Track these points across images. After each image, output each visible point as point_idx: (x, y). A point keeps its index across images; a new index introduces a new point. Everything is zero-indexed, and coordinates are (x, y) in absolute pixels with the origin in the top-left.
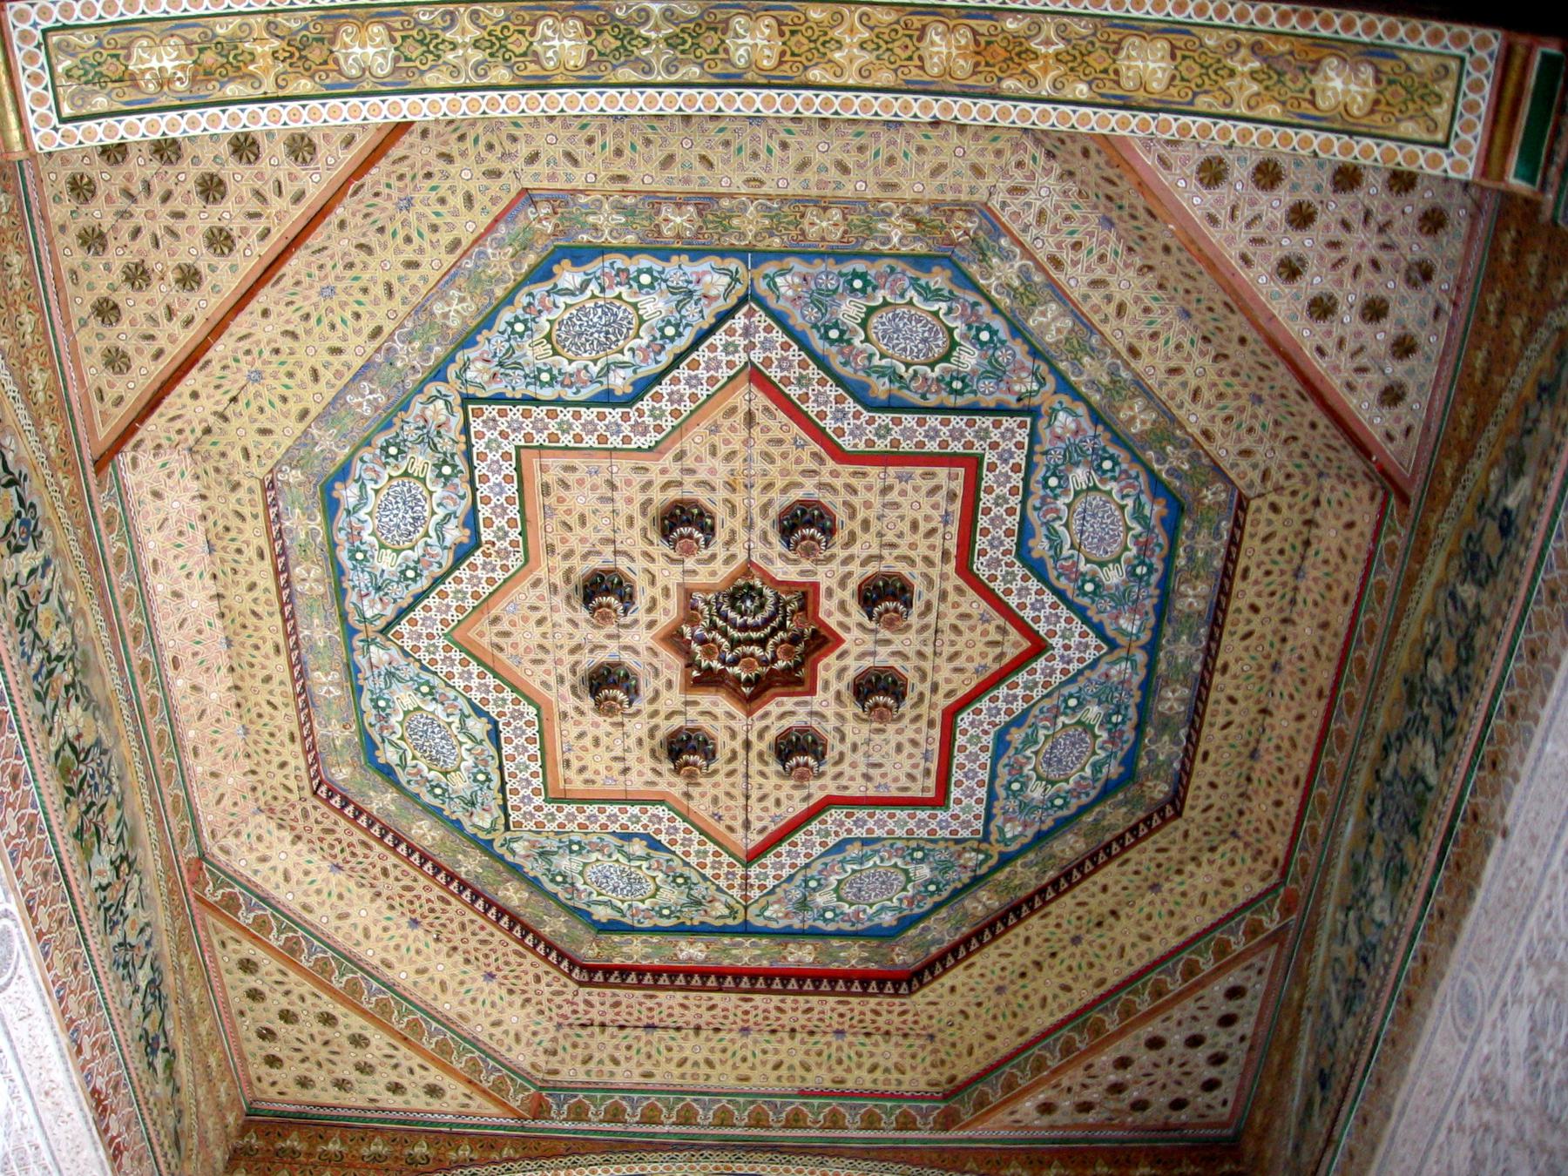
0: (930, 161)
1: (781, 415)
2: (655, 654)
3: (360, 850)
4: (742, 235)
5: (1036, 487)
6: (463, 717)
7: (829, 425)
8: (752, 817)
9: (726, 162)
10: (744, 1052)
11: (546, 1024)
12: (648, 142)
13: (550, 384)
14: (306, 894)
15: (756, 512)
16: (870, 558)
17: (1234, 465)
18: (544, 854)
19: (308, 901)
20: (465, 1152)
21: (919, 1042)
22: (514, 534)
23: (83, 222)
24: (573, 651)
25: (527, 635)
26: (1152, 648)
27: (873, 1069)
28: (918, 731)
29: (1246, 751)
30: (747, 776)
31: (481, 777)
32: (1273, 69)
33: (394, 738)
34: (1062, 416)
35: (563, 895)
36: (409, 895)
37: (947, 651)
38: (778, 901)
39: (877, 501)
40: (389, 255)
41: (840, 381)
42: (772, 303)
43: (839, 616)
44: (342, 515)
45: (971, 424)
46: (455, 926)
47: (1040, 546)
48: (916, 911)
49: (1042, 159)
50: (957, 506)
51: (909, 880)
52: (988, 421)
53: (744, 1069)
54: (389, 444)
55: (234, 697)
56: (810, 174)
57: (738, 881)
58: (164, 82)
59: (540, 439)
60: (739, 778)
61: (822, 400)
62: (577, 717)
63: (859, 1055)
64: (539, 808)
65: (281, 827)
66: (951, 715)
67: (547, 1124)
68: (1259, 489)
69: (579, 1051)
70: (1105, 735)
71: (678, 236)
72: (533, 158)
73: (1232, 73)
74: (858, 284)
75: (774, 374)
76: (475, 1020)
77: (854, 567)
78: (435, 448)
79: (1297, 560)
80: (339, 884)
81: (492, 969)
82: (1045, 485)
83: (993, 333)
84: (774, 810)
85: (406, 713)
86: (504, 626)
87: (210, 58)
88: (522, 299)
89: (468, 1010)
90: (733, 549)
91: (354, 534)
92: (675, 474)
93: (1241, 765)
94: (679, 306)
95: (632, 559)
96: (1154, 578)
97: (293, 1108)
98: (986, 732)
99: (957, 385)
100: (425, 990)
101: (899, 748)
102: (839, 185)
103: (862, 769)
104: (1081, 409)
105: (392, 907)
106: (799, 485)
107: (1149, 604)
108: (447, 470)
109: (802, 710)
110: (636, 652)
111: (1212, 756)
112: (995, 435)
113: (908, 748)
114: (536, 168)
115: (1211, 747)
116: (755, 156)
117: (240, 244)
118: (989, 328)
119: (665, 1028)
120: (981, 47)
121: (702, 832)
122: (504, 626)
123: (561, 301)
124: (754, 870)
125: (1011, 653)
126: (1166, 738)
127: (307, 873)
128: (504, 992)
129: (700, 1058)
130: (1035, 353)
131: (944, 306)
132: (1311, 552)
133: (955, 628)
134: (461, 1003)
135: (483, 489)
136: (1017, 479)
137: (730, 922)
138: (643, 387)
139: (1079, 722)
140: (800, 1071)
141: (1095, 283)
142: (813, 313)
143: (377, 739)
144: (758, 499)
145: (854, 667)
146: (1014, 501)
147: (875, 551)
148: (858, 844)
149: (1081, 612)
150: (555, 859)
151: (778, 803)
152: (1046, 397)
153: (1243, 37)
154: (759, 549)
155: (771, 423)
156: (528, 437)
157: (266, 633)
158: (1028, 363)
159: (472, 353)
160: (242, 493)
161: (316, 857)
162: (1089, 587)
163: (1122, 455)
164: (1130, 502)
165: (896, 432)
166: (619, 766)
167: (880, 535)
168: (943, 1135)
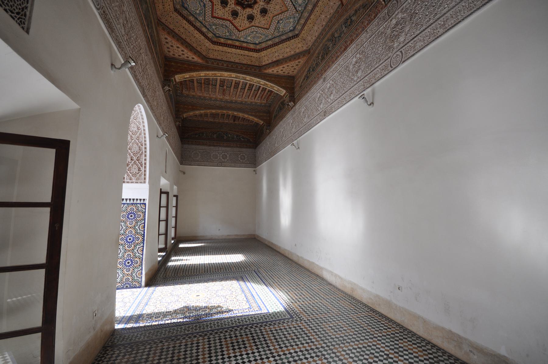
1: (237, 26)
7: (231, 24)
22: (273, 21)
24: (272, 3)
39: (225, 14)
44: (294, 26)
47: (202, 4)
50: (214, 11)
61: (231, 27)
75: (237, 31)
86: (280, 9)
91: (293, 24)
104: (199, 20)
112: (210, 19)
122: (280, 9)
135: (275, 26)
136: (206, 14)
142: (232, 34)
144: (241, 17)
146: (206, 11)
160: (302, 36)
163: (192, 13)
165: (223, 22)
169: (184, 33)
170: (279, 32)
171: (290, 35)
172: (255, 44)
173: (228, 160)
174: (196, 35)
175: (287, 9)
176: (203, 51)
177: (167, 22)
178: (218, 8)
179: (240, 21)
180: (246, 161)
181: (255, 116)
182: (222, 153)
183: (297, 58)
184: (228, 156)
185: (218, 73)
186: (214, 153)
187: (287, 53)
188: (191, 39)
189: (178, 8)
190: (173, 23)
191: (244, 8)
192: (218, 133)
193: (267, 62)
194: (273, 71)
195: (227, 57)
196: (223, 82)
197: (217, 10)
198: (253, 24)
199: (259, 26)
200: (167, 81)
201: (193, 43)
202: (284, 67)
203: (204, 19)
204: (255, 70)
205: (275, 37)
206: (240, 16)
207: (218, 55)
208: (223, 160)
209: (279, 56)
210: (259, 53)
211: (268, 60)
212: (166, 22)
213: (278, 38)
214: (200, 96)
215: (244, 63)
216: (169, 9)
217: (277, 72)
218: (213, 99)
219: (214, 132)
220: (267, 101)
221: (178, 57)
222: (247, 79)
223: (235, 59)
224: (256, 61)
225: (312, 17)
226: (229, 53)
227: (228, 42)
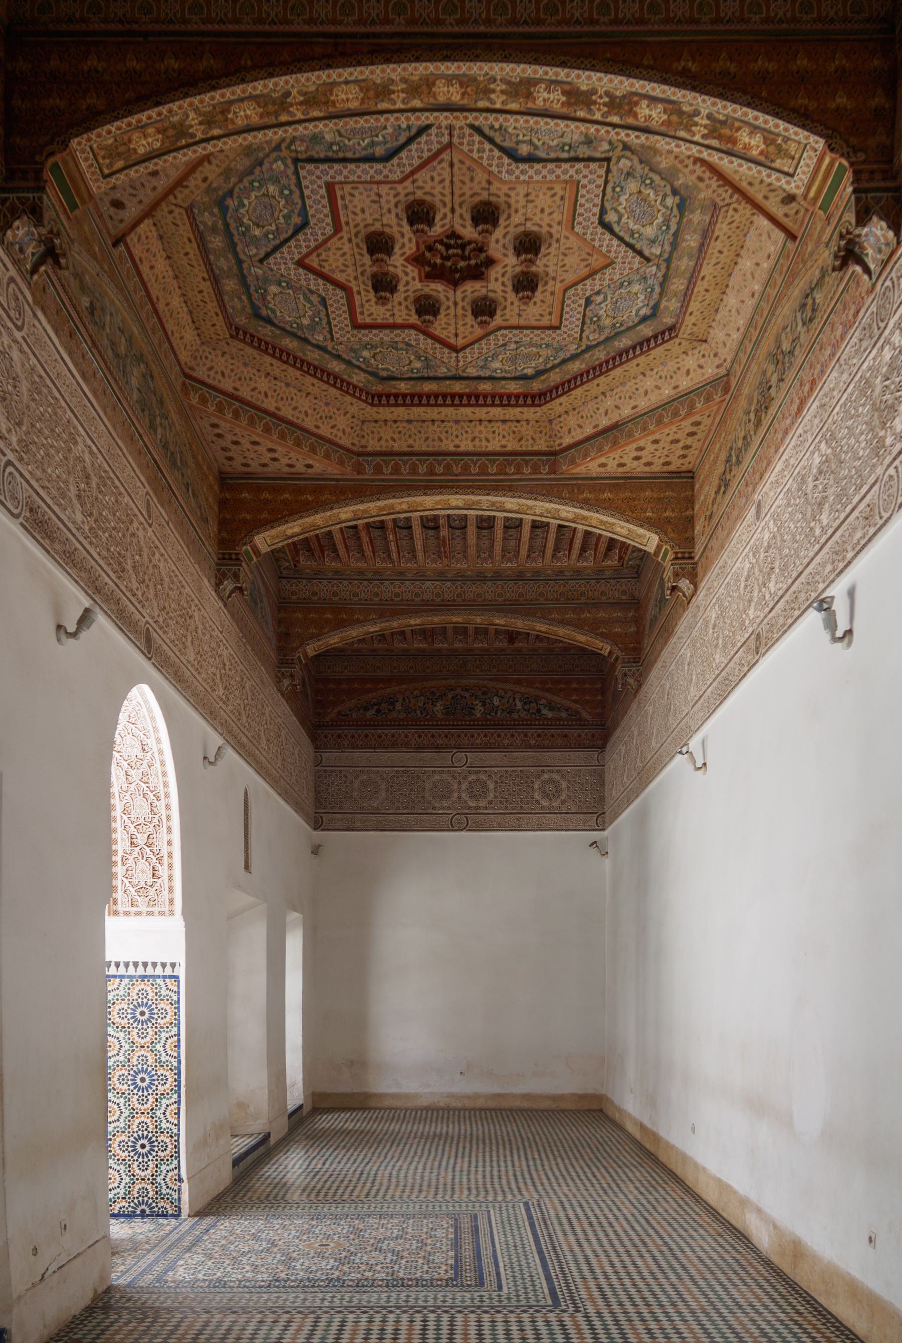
8: (448, 170)
22: (568, 302)
28: (354, 220)
62: (552, 223)
64: (585, 177)
70: (245, 220)
86: (583, 264)
88: (549, 366)
101: (363, 211)
104: (314, 341)
113: (358, 210)
122: (583, 264)
136: (334, 323)
139: (263, 227)
151: (432, 179)
152: (329, 345)
163: (289, 329)
170: (601, 329)
172: (524, 377)
173: (491, 802)
174: (310, 389)
176: (340, 434)
179: (452, 322)
180: (563, 802)
181: (578, 625)
182: (465, 778)
183: (683, 413)
184: (491, 786)
185: (401, 504)
186: (437, 777)
188: (294, 404)
190: (232, 370)
191: (455, 284)
192: (450, 696)
193: (578, 435)
194: (603, 465)
195: (427, 439)
196: (431, 524)
198: (498, 320)
199: (522, 322)
200: (230, 559)
202: (641, 449)
203: (329, 336)
204: (536, 470)
205: (589, 348)
207: (396, 436)
208: (472, 804)
210: (545, 408)
211: (580, 426)
213: (602, 347)
214: (361, 572)
215: (490, 448)
217: (621, 465)
218: (410, 576)
219: (433, 693)
220: (621, 558)
221: (260, 469)
224: (538, 436)
225: (706, 270)
226: (433, 421)
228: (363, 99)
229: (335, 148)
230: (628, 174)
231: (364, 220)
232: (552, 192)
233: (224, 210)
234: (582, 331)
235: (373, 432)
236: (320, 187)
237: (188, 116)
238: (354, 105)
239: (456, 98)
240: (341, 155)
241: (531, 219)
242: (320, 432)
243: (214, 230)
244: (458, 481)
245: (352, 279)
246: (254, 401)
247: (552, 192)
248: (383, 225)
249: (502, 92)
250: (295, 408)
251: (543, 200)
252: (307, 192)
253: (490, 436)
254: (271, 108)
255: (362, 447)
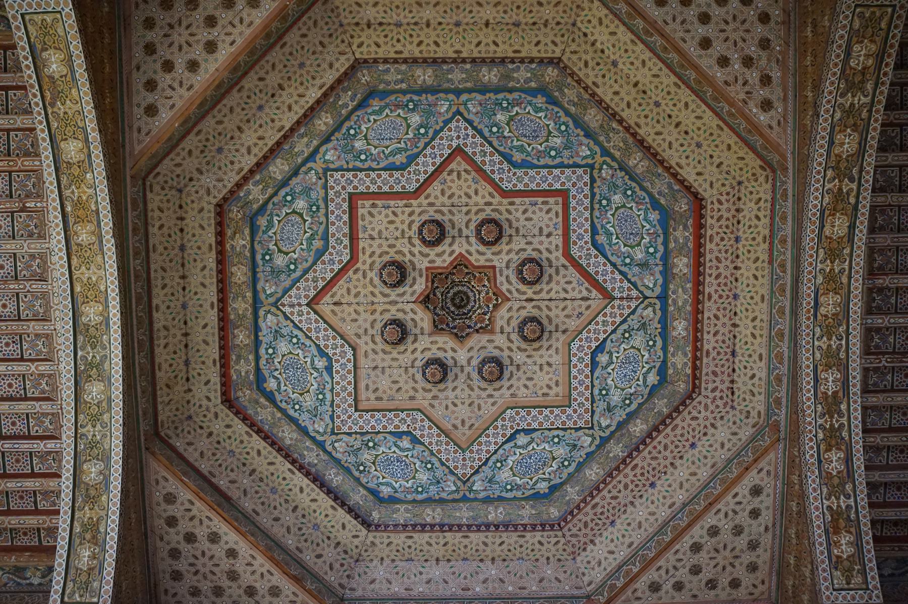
0: (198, 231)
1: (334, 290)
2: (472, 348)
3: (599, 510)
4: (246, 309)
5: (366, 165)
6: (516, 446)
7: (337, 267)
8: (580, 296)
9: (204, 318)
10: (748, 298)
11: (730, 415)
12: (198, 351)
13: (324, 395)
14: (622, 544)
15: (386, 300)
16: (410, 243)
17: (338, 70)
18: (609, 409)
19: (627, 543)
20: (795, 479)
21: (743, 191)
22: (403, 415)
23: (209, 594)
24: (472, 390)
25: (463, 411)
26: (458, 93)
27: (758, 218)
28: (517, 210)
29: (514, 29)
30: (550, 300)
31: (556, 440)
32: (58, 96)
33: (531, 483)
34: (327, 157)
35: (640, 400)
36: (631, 487)
37: (464, 199)
38: (642, 279)
40: (255, 462)
41: (314, 263)
42: (279, 295)
43: (446, 256)
44: (397, 495)
45: (333, 200)
46: (654, 463)
47: (400, 159)
48: (647, 200)
49: (194, 183)
50: (379, 203)
51: (624, 206)
52: (331, 193)
53: (758, 298)
54: (358, 470)
55: (499, 562)
56: (207, 282)
57: (625, 303)
58: (93, 557)
59: (351, 400)
60: (552, 304)
61: (324, 271)
63: (750, 227)
64: (575, 411)
65: (585, 550)
66: (504, 194)
67: (783, 424)
68: (350, 55)
69: (747, 398)
70: (516, 108)
71: (249, 337)
72: (208, 399)
73: (65, 113)
74: (267, 257)
75: (312, 293)
76: (717, 459)
77: (416, 250)
78: (360, 449)
79: (392, 27)
80: (622, 524)
81: (687, 444)
82: (366, 160)
83: (287, 194)
84: (574, 285)
85: (514, 475)
86: (458, 423)
87: (88, 536)
88: (283, 405)
89: (710, 462)
90: (408, 310)
91: (408, 491)
92: (368, 339)
93: (523, 30)
94: (283, 336)
95: (416, 359)
96: (415, 98)
97: (774, 578)
98: (515, 174)
99: (314, 208)
100: (693, 485)
102: (211, 269)
103: (543, 238)
104: (323, 149)
105: (641, 496)
106: (371, 279)
107: (431, 98)
108: (371, 444)
109: (505, 272)
110: (472, 357)
111: (516, 48)
113: (529, 214)
114: (212, 398)
115: (510, 50)
116: (201, 306)
117: (214, 529)
118: (285, 197)
119: (734, 345)
120: (79, 220)
121: (590, 323)
122: (458, 423)
123: (283, 388)
124: (617, 294)
125: (464, 166)
126: (515, 75)
127: (612, 541)
128: (705, 438)
129: (751, 325)
130: (296, 173)
131: (275, 218)
132: (384, 21)
133: (450, 197)
134: (705, 465)
135: (379, 428)
136: (361, 175)
137: (658, 307)
138: (322, 353)
139: (508, 124)
140: (759, 264)
141: (249, 152)
142: (283, 277)
143: (532, 492)
145: (476, 246)
146: (373, 175)
147: (406, 240)
148: (597, 237)
149: (436, 133)
150: (613, 404)
151: (569, 283)
153: (50, 111)
154: (406, 297)
155: (339, 294)
156: (350, 406)
157: (456, 541)
158: (301, 176)
159: (310, 429)
160: (377, 541)
161: (605, 534)
162: (422, 131)
163: (347, 124)
164: (372, 118)
166: (546, 368)
167: (397, 238)
168: (790, 171)
169: (261, 84)
170: (356, 452)
171: (358, 497)
172: (260, 379)
175: (464, 446)
176: (178, 160)
177: (311, 23)
178: (394, 214)
187: (277, 519)
189: (359, 74)
193: (192, 455)
195: (164, 270)
197: (389, 212)
199: (362, 373)
201: (219, 117)
205: (321, 445)
206: (385, 296)
209: (245, 492)
212: (310, 18)
216: (356, 41)
222: (94, 391)
223: (163, 308)
227: (234, 269)
228: (830, 238)
229: (604, 202)
230: (575, 446)
231: (518, 220)
232: (553, 386)
233: (534, 92)
234: (349, 434)
235: (168, 201)
236: (563, 184)
237: (865, 96)
238: (827, 231)
239: (823, 310)
240: (597, 206)
241: (518, 370)
242: (192, 136)
243: (507, 77)
244: (131, 313)
245: (431, 200)
246: (263, 62)
247: (553, 386)
248: (510, 236)
249: (830, 346)
250: (231, 110)
251: (543, 379)
252: (556, 172)
253: (171, 348)
254: (843, 165)
255: (151, 186)
